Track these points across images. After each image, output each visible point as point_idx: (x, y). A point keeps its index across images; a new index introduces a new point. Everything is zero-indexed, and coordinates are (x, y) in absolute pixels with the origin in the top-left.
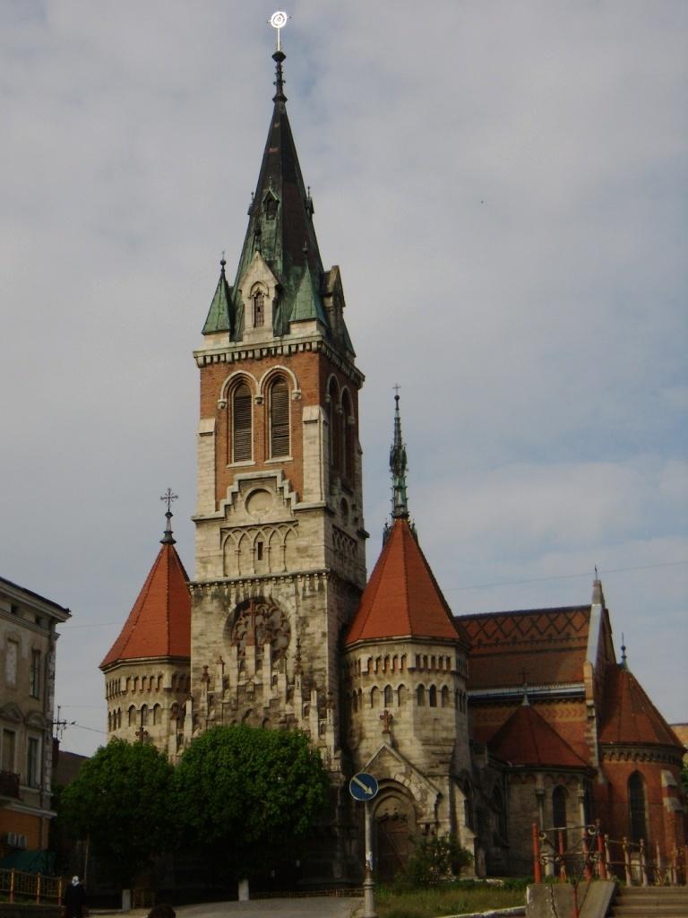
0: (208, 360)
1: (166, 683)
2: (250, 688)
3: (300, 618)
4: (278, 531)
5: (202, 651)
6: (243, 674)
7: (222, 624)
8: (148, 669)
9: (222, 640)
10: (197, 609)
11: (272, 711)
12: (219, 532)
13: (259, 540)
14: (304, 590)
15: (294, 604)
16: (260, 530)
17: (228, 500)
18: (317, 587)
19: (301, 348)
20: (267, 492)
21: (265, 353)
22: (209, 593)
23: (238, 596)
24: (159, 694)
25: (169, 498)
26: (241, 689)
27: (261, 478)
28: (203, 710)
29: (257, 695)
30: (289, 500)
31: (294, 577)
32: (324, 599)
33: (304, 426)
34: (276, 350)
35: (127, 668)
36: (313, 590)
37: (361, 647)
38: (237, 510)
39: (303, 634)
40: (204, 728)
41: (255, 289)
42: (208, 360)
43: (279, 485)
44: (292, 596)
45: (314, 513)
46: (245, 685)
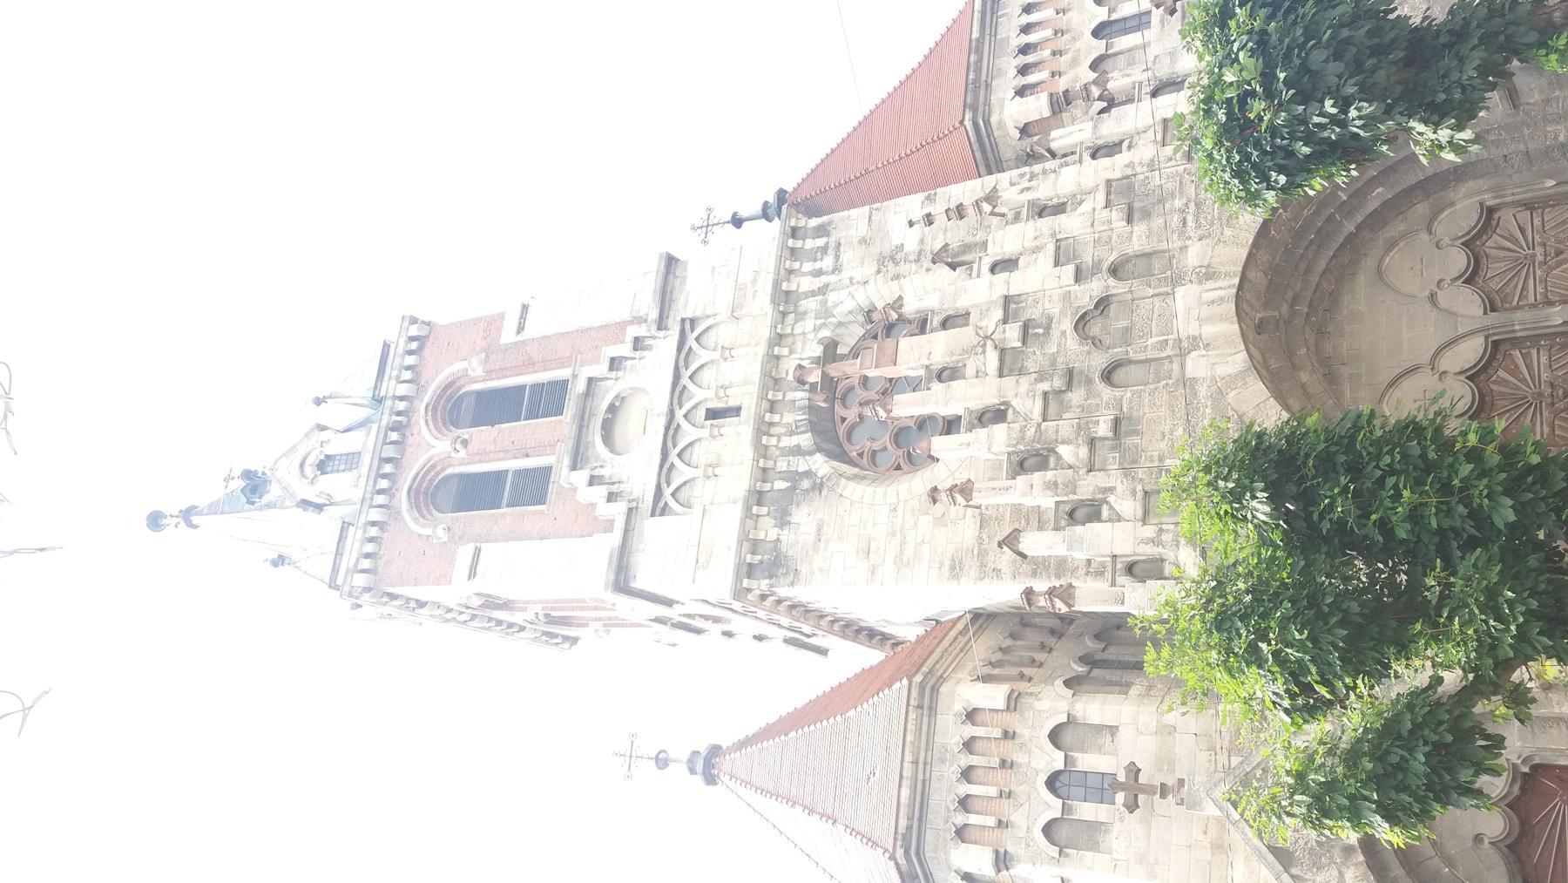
0: (366, 564)
1: (992, 696)
2: (1012, 334)
3: (879, 272)
4: (693, 368)
5: (910, 548)
6: (970, 371)
7: (853, 490)
8: (943, 761)
9: (892, 489)
10: (803, 569)
11: (1087, 259)
12: (657, 519)
13: (701, 413)
14: (818, 273)
15: (844, 293)
16: (679, 414)
17: (601, 491)
18: (821, 242)
19: (411, 360)
20: (612, 409)
21: (394, 436)
22: (773, 534)
23: (798, 451)
24: (1023, 731)
25: (631, 756)
26: (1009, 364)
27: (582, 418)
28: (1052, 486)
29: (1034, 313)
30: (638, 343)
31: (785, 301)
32: (849, 216)
33: (525, 335)
34: (399, 414)
35: (929, 836)
36: (824, 249)
37: (987, 122)
38: (624, 478)
39: (917, 261)
40: (1112, 478)
41: (308, 470)
42: (366, 564)
43: (600, 369)
44: (824, 302)
45: (678, 282)
46: (1003, 352)
